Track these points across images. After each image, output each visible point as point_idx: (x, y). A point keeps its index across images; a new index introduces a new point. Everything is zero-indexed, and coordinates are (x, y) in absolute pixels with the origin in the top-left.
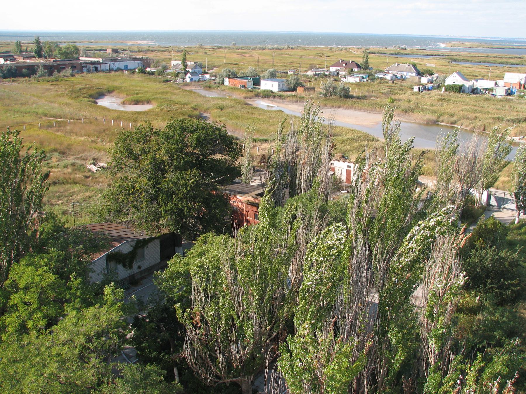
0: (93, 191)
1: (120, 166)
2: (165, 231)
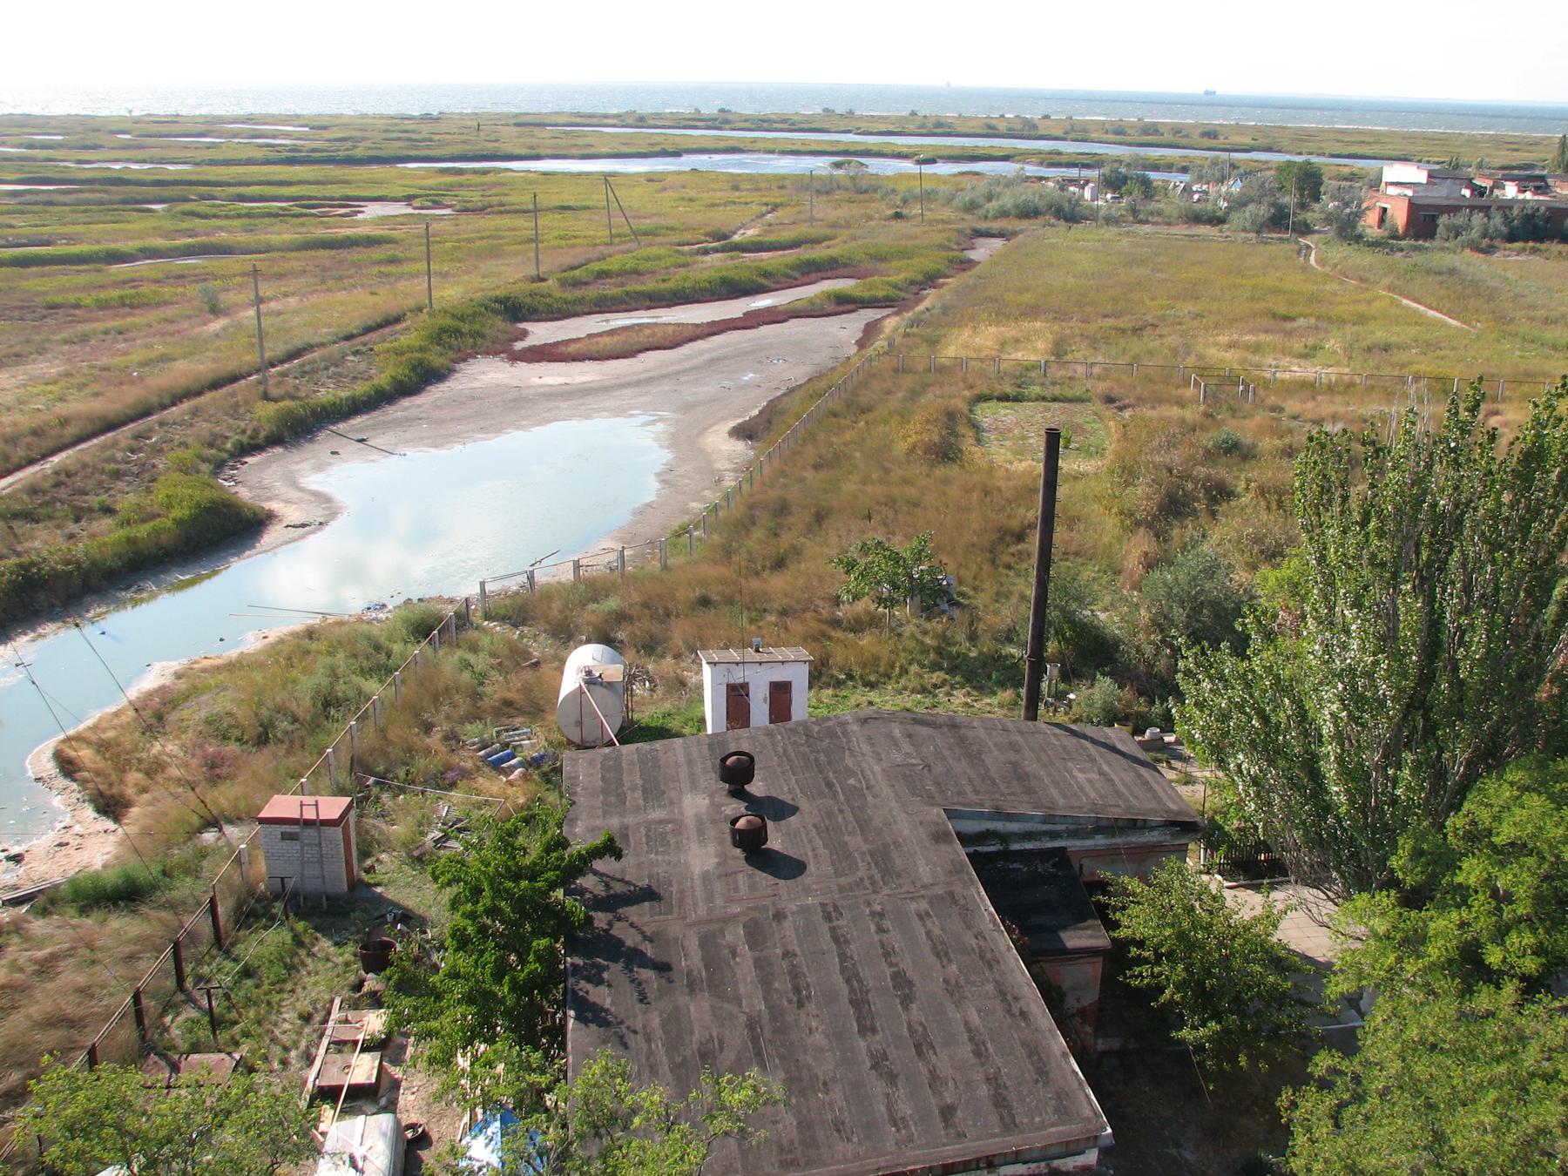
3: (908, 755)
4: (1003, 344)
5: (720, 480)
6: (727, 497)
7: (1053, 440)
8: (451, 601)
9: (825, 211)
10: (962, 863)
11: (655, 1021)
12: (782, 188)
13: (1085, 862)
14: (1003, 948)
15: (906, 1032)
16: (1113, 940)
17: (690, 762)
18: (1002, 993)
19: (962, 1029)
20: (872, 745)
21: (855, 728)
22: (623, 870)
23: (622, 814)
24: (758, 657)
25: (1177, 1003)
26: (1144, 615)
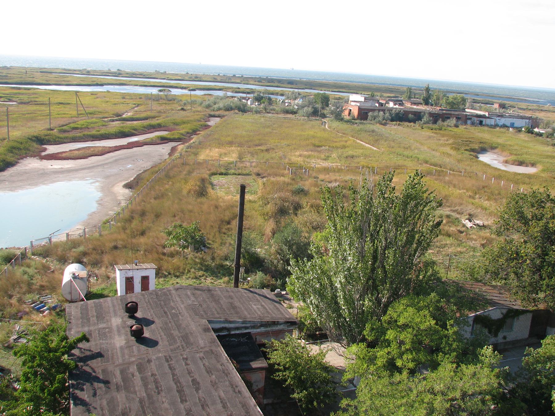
0: (465, 247)
1: (505, 227)
2: (541, 306)
3: (193, 301)
4: (221, 155)
5: (120, 203)
6: (123, 210)
7: (243, 188)
8: (19, 249)
9: (156, 107)
10: (214, 339)
11: (105, 403)
12: (141, 98)
13: (257, 337)
14: (231, 369)
15: (198, 401)
16: (269, 364)
17: (114, 306)
18: (232, 385)
19: (218, 398)
20: (180, 298)
21: (174, 292)
22: (90, 347)
23: (89, 326)
24: (136, 267)
25: (292, 385)
26: (273, 250)
